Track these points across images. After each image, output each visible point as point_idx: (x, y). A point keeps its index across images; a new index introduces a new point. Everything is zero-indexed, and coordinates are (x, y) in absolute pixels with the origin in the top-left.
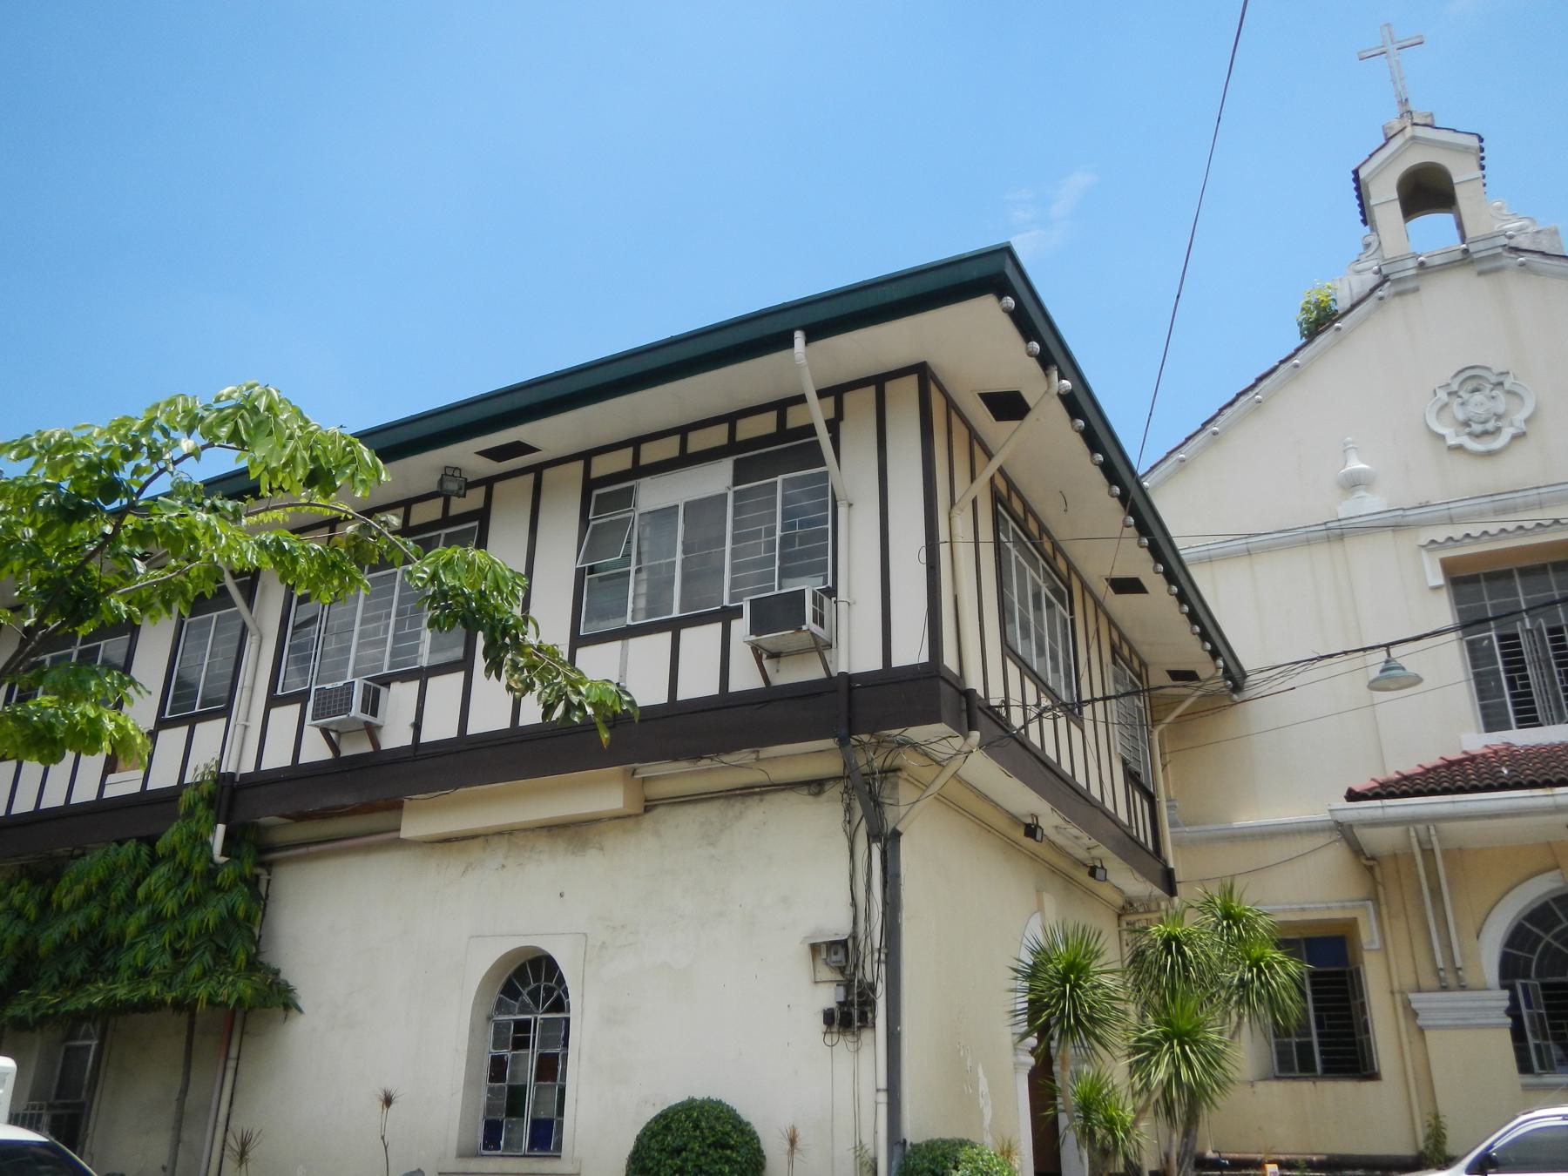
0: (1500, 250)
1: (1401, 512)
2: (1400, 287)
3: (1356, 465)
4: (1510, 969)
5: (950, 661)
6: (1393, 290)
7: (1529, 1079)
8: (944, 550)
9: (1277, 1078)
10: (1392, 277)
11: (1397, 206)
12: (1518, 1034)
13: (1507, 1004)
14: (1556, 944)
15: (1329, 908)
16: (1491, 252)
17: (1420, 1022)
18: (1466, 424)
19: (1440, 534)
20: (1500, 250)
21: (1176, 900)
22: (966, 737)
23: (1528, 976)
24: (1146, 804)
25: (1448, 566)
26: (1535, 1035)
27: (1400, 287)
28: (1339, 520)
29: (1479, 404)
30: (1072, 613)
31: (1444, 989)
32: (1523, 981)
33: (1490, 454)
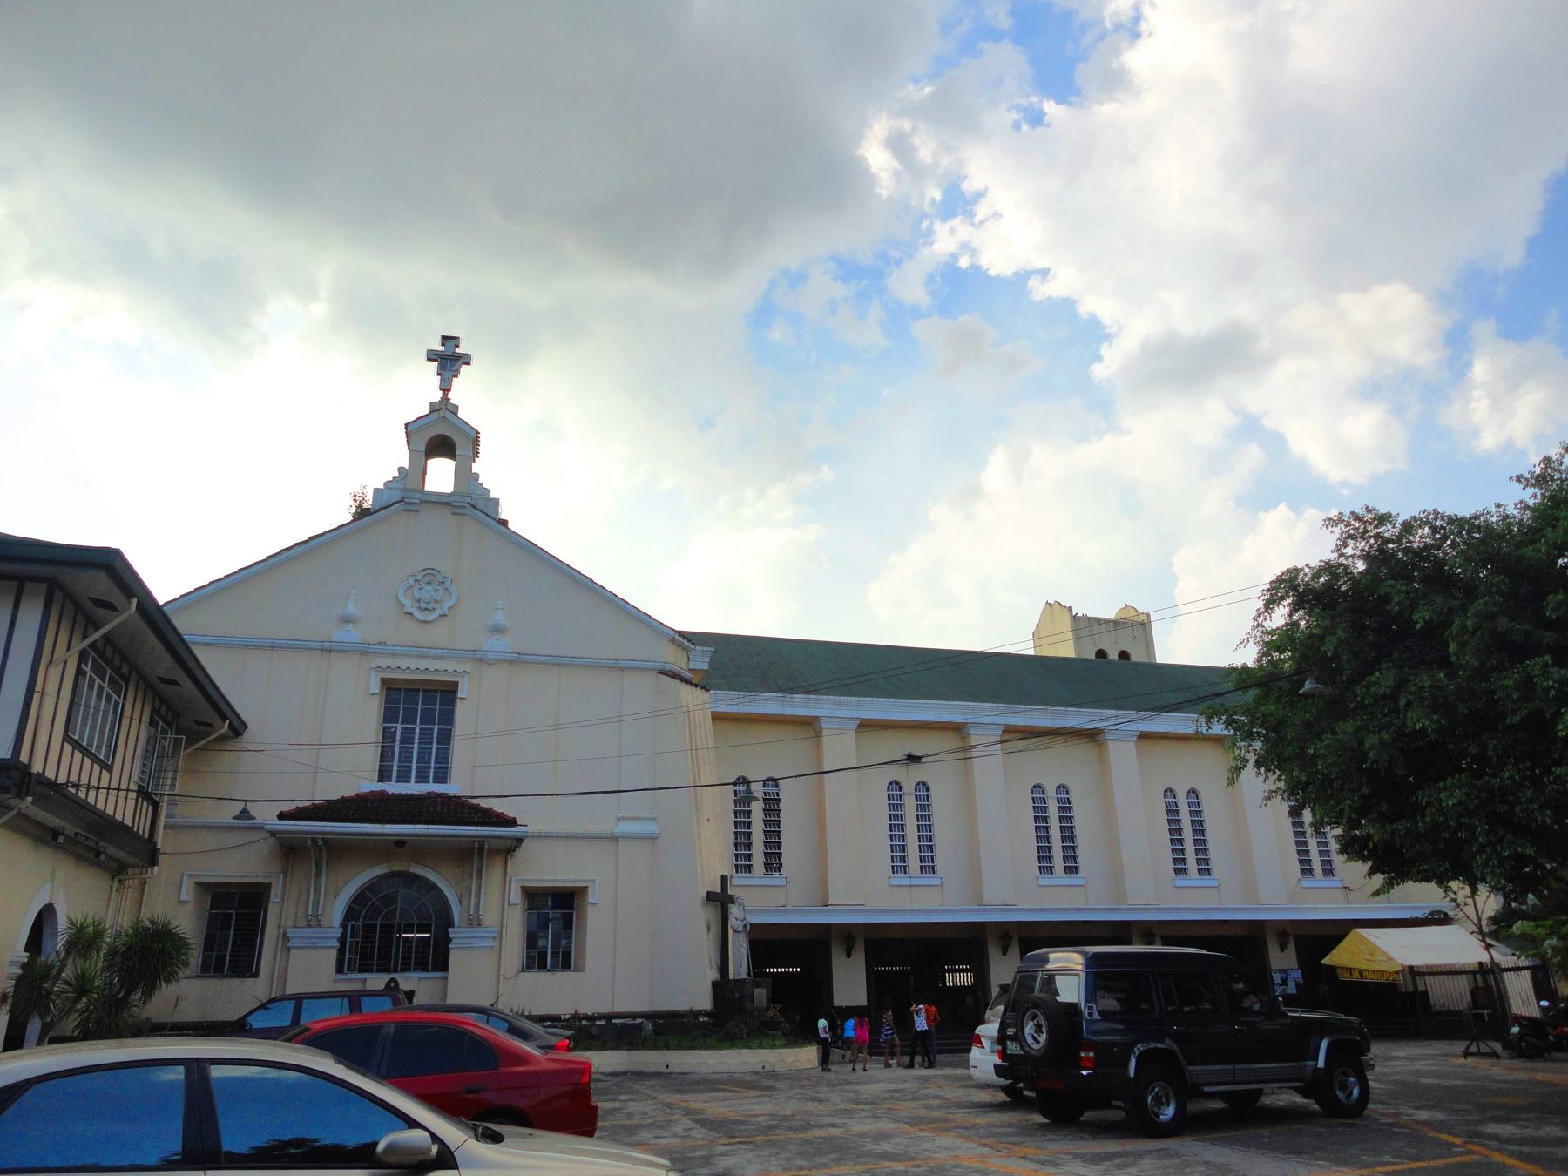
0: (466, 505)
1: (367, 646)
2: (408, 507)
3: (351, 608)
4: (350, 914)
5: (24, 758)
6: (404, 507)
7: (341, 976)
8: (36, 696)
9: (198, 977)
10: (406, 500)
11: (424, 454)
12: (341, 952)
13: (339, 935)
14: (378, 903)
15: (257, 876)
16: (462, 504)
17: (289, 945)
18: (419, 601)
19: (385, 662)
20: (466, 505)
21: (156, 868)
22: (23, 800)
23: (357, 920)
24: (151, 808)
25: (384, 681)
26: (350, 953)
27: (408, 507)
28: (331, 642)
29: (428, 592)
30: (124, 699)
31: (309, 926)
32: (353, 923)
33: (426, 622)
